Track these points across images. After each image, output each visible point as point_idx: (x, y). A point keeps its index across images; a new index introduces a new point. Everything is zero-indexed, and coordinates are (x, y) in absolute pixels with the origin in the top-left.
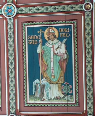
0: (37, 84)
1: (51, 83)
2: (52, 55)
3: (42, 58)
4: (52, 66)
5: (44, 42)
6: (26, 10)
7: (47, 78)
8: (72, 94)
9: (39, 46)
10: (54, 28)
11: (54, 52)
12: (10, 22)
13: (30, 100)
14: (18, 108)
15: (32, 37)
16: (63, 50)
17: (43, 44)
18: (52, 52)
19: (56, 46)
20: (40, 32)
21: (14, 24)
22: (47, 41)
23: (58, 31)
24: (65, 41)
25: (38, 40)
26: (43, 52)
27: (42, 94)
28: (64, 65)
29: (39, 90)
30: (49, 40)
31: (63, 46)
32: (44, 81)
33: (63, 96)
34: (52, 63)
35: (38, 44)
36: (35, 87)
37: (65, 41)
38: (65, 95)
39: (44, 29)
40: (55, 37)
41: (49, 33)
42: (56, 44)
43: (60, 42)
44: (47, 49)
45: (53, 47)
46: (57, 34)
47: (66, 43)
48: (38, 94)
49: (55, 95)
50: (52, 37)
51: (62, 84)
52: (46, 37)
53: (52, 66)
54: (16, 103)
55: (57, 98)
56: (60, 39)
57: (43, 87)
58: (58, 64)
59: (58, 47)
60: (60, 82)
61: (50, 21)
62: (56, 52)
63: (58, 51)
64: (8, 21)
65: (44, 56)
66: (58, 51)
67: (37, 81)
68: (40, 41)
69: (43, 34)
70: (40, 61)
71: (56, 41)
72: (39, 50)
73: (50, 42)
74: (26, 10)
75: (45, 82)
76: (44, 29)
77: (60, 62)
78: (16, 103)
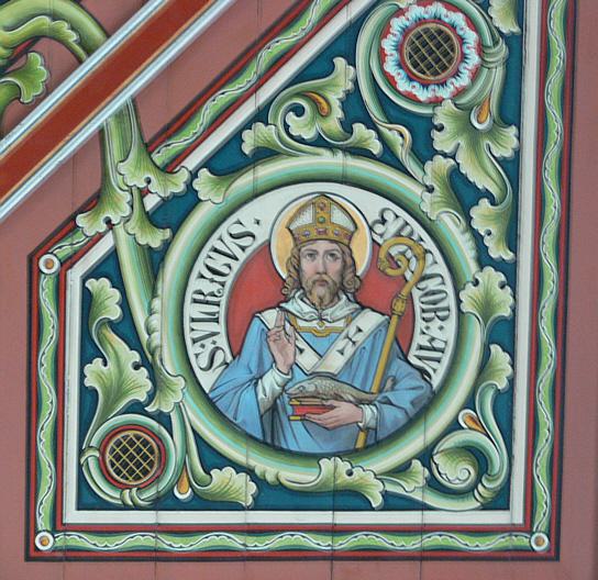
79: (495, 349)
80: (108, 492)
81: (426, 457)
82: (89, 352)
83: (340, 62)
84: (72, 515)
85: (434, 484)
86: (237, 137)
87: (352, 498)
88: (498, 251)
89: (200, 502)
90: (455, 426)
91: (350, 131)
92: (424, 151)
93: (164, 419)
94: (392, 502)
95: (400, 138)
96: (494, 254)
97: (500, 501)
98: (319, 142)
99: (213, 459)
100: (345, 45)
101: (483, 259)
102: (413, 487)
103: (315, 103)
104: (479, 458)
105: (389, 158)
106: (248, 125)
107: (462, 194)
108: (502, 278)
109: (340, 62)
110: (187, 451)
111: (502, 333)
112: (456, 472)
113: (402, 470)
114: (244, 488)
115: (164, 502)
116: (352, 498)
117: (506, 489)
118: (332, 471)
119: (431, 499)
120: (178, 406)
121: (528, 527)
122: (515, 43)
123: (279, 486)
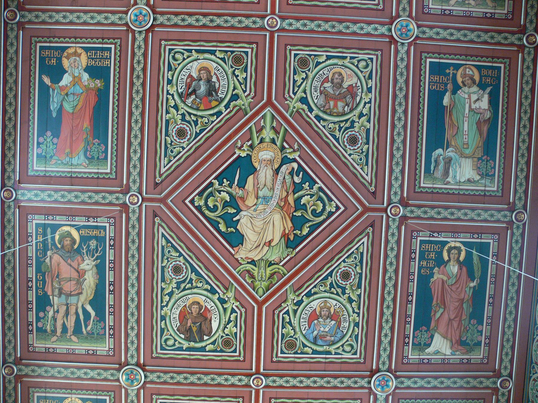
0: (439, 156)
1: (463, 155)
2: (467, 111)
3: (450, 115)
4: (466, 128)
5: (456, 88)
6: (430, 33)
7: (456, 147)
8: (494, 175)
9: (447, 94)
10: (473, 68)
11: (470, 106)
12: (403, 50)
13: (425, 184)
14: (405, 195)
15: (436, 78)
16: (484, 104)
17: (454, 92)
18: (467, 106)
19: (474, 97)
20: (451, 71)
21: (408, 52)
22: (460, 88)
23: (480, 73)
24: (488, 90)
25: (446, 85)
26: (453, 104)
27: (446, 173)
28: (485, 129)
29: (441, 167)
30: (465, 85)
31: (486, 98)
32: (450, 153)
33: (478, 177)
34: (466, 124)
35: (446, 91)
36: (436, 161)
37: (488, 90)
38: (482, 176)
39: (457, 67)
40: (474, 82)
41: (464, 75)
42: (474, 93)
43: (481, 92)
44: (459, 101)
45: (470, 98)
46: (477, 78)
47: (490, 94)
48: (439, 173)
49: (467, 176)
50: (470, 82)
51: (479, 159)
52: (459, 80)
53: (466, 128)
54: (402, 186)
55: (469, 180)
56: (482, 86)
57: (448, 162)
58: (475, 126)
59: (478, 99)
60: (476, 155)
61: (468, 54)
62: (473, 106)
63: (477, 105)
64: (400, 48)
65: (454, 112)
66: (477, 105)
67: (440, 151)
68: (450, 86)
69: (455, 75)
70: (447, 119)
71: (475, 89)
72: (446, 101)
73: (466, 89)
74: (430, 33)
75: (451, 154)
76: (457, 67)
77: (479, 123)
78: (402, 186)
79: (171, 79)
80: (242, 54)
81: (184, 59)
82: (246, 79)
83: (198, 132)
84: (249, 50)
85: (183, 54)
86: (217, 118)
87: (197, 51)
88: (170, 97)
89: (226, 52)
90: (179, 64)
91: (196, 119)
92: (183, 115)
93: (232, 67)
94: (190, 51)
95: (187, 118)
96: (171, 96)
97: (170, 50)
98: (202, 117)
99: (223, 59)
100: (197, 135)
101: (173, 95)
102: (186, 54)
103: (203, 123)
104: (174, 59)
105: (190, 114)
106: (215, 120)
107: (176, 107)
108: (169, 92)
109: (198, 132)
110: (228, 60)
111: (170, 82)
112: (178, 56)
113: (188, 57)
114: (217, 53)
115: (232, 52)
116: (197, 51)
117: (169, 53)
118: (201, 56)
119: (182, 51)
120: (229, 69)
121: (165, 45)
122: (167, 135)
123: (212, 54)
